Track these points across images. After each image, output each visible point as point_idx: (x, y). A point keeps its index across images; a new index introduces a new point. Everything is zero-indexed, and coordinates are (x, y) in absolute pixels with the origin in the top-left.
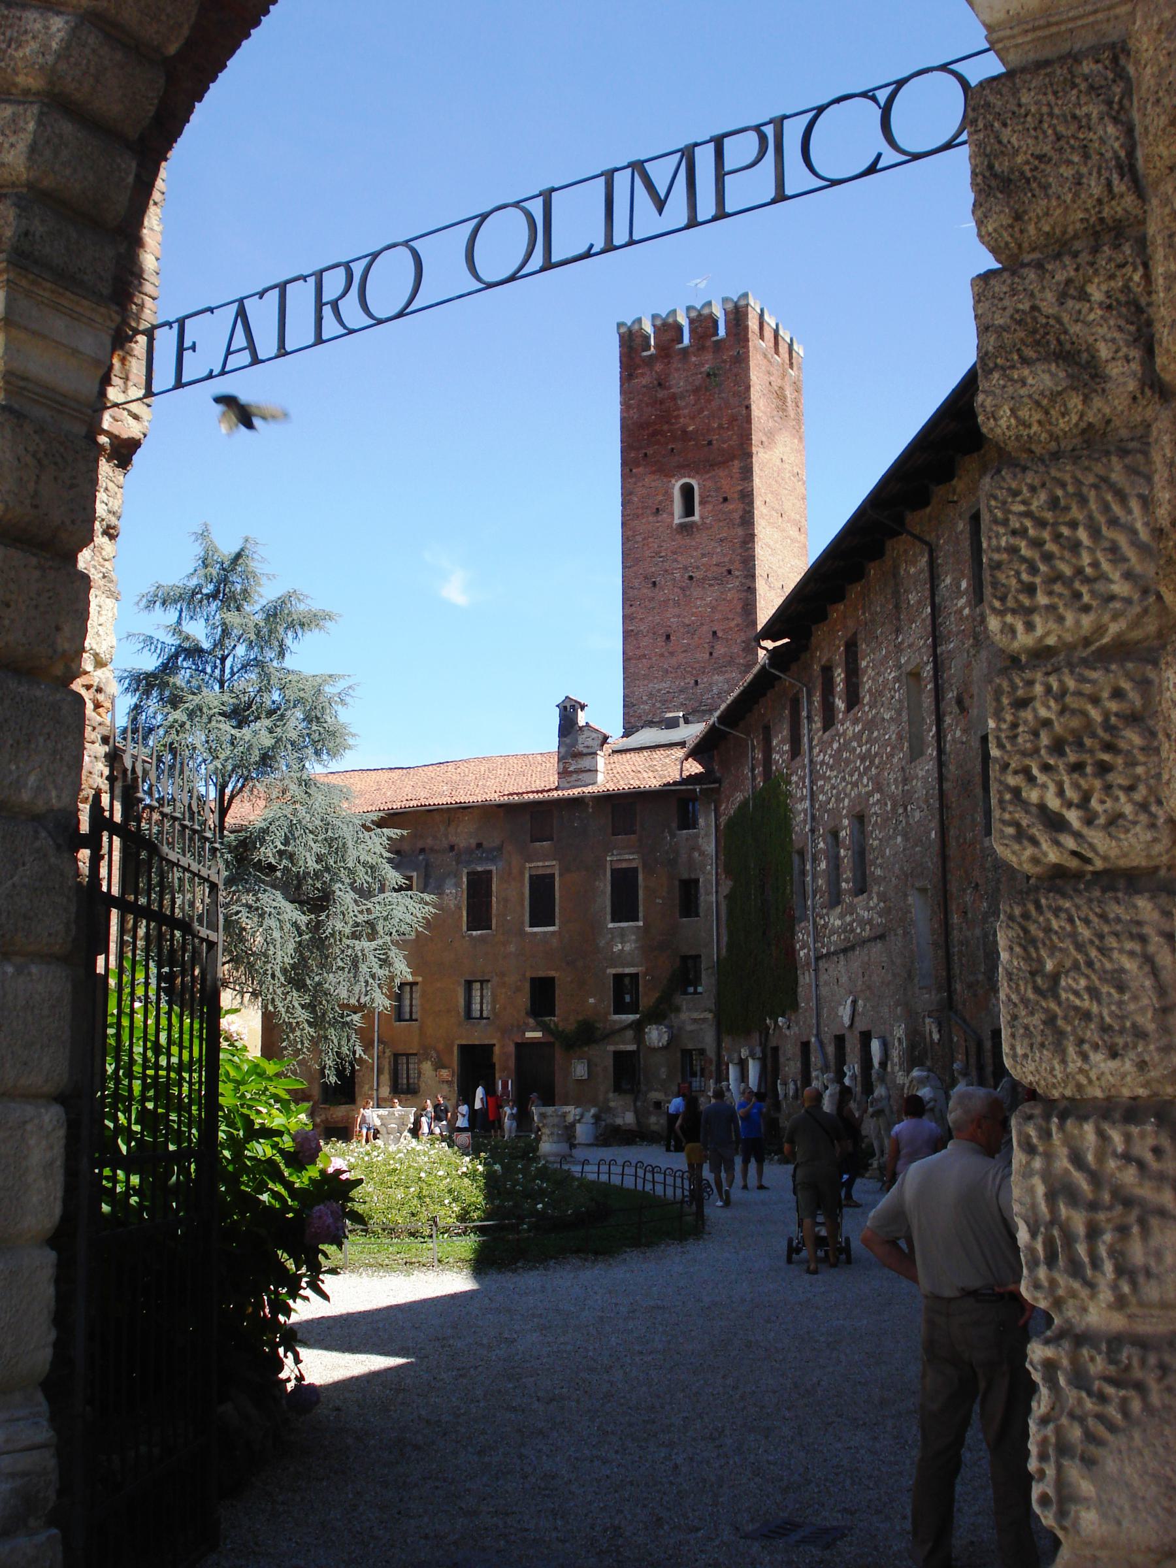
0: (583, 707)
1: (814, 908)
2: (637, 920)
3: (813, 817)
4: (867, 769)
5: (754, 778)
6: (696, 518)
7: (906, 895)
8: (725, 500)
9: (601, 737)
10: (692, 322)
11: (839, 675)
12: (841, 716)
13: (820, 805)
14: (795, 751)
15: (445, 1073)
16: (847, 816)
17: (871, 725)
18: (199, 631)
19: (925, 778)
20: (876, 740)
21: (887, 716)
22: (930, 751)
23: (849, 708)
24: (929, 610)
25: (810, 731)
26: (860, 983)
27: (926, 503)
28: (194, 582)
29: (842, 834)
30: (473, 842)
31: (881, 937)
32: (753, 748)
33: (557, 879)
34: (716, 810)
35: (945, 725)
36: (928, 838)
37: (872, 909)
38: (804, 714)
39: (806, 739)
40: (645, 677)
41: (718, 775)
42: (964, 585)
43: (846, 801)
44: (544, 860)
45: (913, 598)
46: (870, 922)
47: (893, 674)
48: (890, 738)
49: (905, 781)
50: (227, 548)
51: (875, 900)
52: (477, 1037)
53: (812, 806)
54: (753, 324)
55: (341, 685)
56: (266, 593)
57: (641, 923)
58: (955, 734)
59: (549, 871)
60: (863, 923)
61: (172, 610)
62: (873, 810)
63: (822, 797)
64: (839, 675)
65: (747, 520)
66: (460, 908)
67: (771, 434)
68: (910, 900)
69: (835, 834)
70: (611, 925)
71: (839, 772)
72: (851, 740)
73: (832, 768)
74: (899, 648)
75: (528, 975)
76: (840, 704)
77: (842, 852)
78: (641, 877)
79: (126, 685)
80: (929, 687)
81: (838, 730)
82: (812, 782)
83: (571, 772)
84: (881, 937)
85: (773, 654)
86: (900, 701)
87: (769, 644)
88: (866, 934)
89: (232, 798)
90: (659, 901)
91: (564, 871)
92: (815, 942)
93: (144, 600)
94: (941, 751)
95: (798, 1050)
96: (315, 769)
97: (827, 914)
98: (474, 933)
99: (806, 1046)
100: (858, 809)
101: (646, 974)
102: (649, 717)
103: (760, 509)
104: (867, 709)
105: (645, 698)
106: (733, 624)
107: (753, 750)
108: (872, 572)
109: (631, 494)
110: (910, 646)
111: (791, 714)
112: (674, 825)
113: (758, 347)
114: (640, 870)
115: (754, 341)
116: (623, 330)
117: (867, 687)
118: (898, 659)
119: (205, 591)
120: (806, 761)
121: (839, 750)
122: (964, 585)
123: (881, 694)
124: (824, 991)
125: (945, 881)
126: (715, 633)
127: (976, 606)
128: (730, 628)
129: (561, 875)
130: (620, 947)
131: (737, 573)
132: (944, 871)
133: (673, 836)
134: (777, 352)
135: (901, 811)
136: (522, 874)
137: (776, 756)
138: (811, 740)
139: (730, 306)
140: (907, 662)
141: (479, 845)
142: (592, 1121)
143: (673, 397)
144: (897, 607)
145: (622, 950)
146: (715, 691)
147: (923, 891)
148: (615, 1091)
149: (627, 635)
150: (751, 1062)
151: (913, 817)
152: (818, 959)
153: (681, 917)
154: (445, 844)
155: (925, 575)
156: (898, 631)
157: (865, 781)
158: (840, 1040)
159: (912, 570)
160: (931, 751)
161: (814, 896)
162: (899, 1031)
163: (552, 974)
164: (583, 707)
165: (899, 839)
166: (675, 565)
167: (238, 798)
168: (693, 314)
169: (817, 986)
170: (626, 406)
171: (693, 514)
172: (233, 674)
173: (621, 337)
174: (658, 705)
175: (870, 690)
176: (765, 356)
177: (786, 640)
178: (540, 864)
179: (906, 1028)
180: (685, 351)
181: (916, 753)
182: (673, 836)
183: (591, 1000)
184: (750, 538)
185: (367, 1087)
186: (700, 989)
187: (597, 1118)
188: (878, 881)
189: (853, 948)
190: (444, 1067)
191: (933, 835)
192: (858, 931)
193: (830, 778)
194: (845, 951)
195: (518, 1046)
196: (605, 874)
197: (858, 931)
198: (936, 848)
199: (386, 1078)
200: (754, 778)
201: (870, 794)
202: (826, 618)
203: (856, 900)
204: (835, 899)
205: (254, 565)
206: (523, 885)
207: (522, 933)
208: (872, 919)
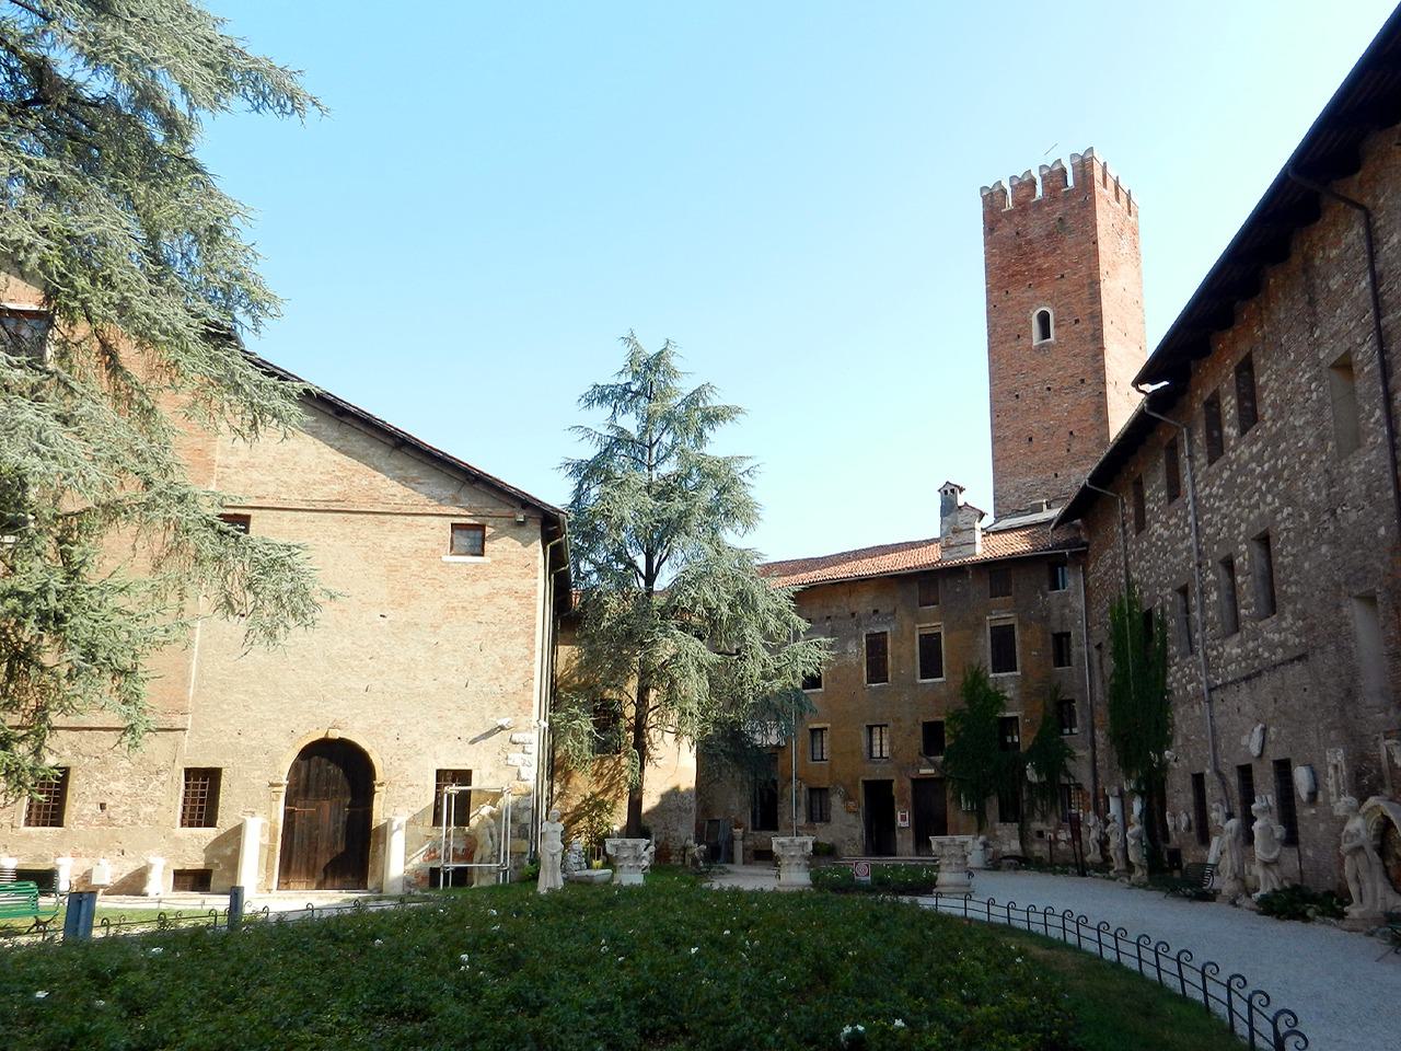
0: (961, 490)
1: (1204, 641)
3: (1200, 552)
4: (1275, 484)
5: (1125, 533)
6: (1052, 339)
7: (1338, 607)
8: (1077, 321)
10: (1044, 178)
11: (1229, 406)
12: (1232, 443)
14: (1174, 490)
16: (1245, 541)
17: (1274, 440)
18: (630, 423)
19: (1366, 473)
20: (1284, 452)
21: (1299, 422)
23: (1243, 431)
25: (1192, 470)
26: (1271, 709)
27: (1356, 169)
28: (623, 380)
29: (1238, 561)
30: (871, 609)
31: (1301, 658)
32: (1123, 505)
33: (943, 637)
37: (1284, 630)
39: (1187, 479)
40: (1011, 474)
41: (1085, 540)
43: (1243, 527)
45: (1335, 283)
46: (1282, 644)
48: (1305, 444)
49: (1331, 483)
50: (650, 349)
51: (1290, 620)
52: (878, 773)
53: (1198, 543)
54: (1098, 175)
55: (747, 465)
56: (685, 386)
57: (1019, 673)
60: (1272, 647)
61: (608, 407)
62: (1282, 526)
64: (1229, 406)
65: (1097, 337)
66: (861, 664)
67: (1114, 265)
70: (992, 675)
71: (1233, 499)
72: (1247, 463)
73: (1221, 499)
74: (1317, 344)
77: (1239, 579)
78: (1017, 633)
79: (570, 470)
82: (1196, 519)
84: (1301, 658)
85: (1153, 399)
87: (1149, 388)
89: (660, 564)
90: (1033, 653)
92: (1208, 673)
93: (583, 400)
95: (1189, 782)
96: (731, 537)
97: (1222, 645)
99: (1198, 780)
100: (1260, 530)
103: (1107, 329)
105: (1012, 491)
106: (1087, 424)
107: (1123, 507)
108: (1272, 281)
111: (1167, 462)
112: (1046, 587)
113: (1103, 195)
114: (1016, 627)
115: (1098, 187)
117: (1268, 401)
119: (634, 388)
121: (1231, 477)
124: (1220, 722)
128: (1084, 428)
131: (1090, 382)
133: (1045, 595)
134: (1118, 199)
137: (1149, 506)
138: (1193, 478)
139: (1077, 160)
141: (876, 612)
142: (982, 847)
143: (1030, 242)
144: (1312, 302)
146: (1073, 481)
147: (1369, 599)
148: (1001, 821)
149: (996, 440)
151: (1346, 519)
152: (1210, 690)
153: (1056, 666)
156: (1313, 326)
157: (1269, 498)
158: (1245, 772)
161: (1204, 629)
162: (1337, 756)
164: (961, 490)
167: (666, 563)
168: (1045, 172)
169: (1211, 717)
170: (989, 256)
171: (1049, 337)
173: (984, 198)
174: (1024, 496)
175: (1273, 405)
177: (1165, 383)
178: (928, 625)
179: (1347, 754)
180: (1039, 204)
182: (1045, 595)
184: (1100, 351)
185: (787, 817)
186: (1075, 730)
187: (985, 845)
188: (1292, 599)
189: (1259, 674)
190: (852, 800)
193: (1219, 508)
194: (1247, 678)
196: (985, 632)
199: (803, 810)
200: (1125, 533)
201: (1276, 512)
202: (1210, 352)
204: (1236, 626)
205: (675, 362)
206: (914, 642)
207: (915, 685)
208: (1286, 640)
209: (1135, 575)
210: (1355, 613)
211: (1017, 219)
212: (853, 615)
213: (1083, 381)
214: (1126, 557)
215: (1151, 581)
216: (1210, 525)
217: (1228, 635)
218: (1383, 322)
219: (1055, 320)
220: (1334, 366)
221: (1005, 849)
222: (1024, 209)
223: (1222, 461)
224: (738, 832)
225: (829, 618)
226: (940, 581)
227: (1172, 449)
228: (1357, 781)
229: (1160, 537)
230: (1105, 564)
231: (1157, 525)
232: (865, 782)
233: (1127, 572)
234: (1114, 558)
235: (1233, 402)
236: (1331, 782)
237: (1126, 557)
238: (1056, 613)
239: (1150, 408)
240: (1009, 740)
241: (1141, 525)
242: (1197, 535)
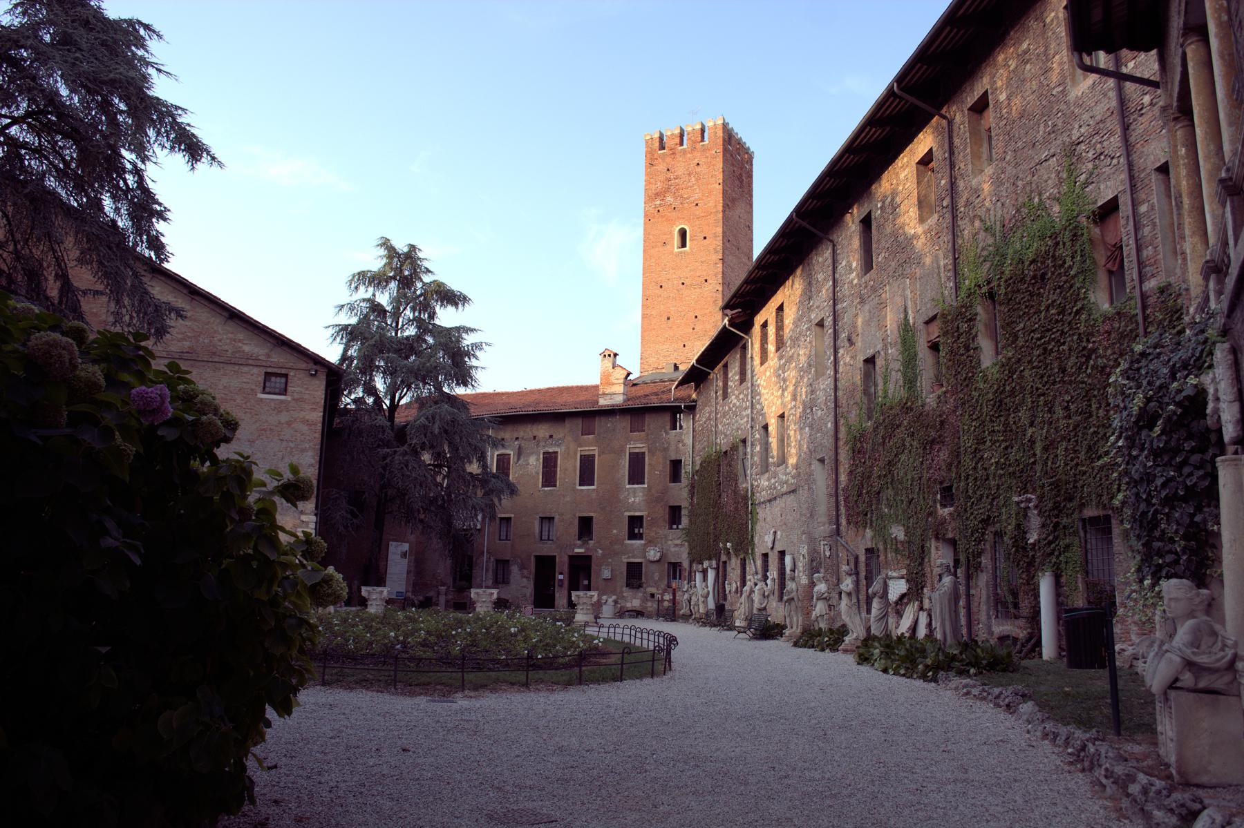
0: (616, 355)
1: (751, 475)
2: (644, 483)
3: (753, 419)
5: (717, 398)
6: (687, 248)
7: (810, 464)
8: (705, 238)
9: (626, 373)
11: (771, 330)
12: (772, 355)
13: (757, 412)
14: (743, 379)
15: (525, 572)
19: (824, 389)
22: (829, 372)
24: (831, 283)
29: (770, 428)
30: (547, 435)
31: (793, 491)
34: (693, 419)
35: (839, 355)
36: (826, 427)
37: (788, 474)
38: (749, 356)
42: (854, 264)
43: (774, 407)
44: (589, 446)
45: (820, 277)
46: (786, 482)
47: (806, 326)
49: (812, 392)
52: (546, 549)
53: (752, 412)
58: (845, 358)
59: (591, 453)
60: (783, 483)
63: (758, 407)
64: (771, 330)
68: (813, 467)
69: (766, 427)
70: (628, 486)
75: (577, 515)
76: (771, 348)
80: (829, 332)
81: (769, 364)
82: (752, 397)
83: (607, 394)
84: (793, 491)
86: (810, 342)
88: (785, 489)
91: (601, 453)
94: (836, 371)
98: (546, 489)
100: (781, 412)
101: (648, 516)
102: (656, 366)
104: (788, 349)
107: (717, 381)
109: (649, 234)
110: (818, 307)
112: (668, 427)
114: (647, 454)
116: (648, 138)
118: (810, 316)
120: (749, 385)
122: (854, 264)
123: (798, 339)
125: (837, 454)
126: (696, 317)
127: (862, 277)
129: (599, 456)
130: (633, 499)
132: (836, 448)
133: (667, 433)
135: (808, 411)
136: (576, 454)
137: (730, 383)
140: (815, 318)
141: (551, 436)
145: (634, 502)
147: (822, 461)
148: (627, 586)
149: (644, 316)
150: (709, 570)
154: (531, 436)
155: (830, 261)
159: (820, 260)
160: (831, 372)
161: (752, 468)
162: (804, 550)
163: (591, 514)
165: (807, 429)
166: (674, 276)
172: (403, 326)
176: (732, 155)
178: (587, 448)
180: (684, 151)
181: (818, 375)
182: (667, 433)
183: (615, 531)
187: (616, 602)
189: (775, 498)
190: (525, 568)
191: (829, 425)
192: (779, 488)
194: (770, 501)
195: (571, 557)
196: (625, 456)
197: (779, 488)
198: (832, 432)
200: (717, 398)
203: (778, 469)
207: (574, 490)
209: (720, 427)
210: (816, 466)
211: (668, 159)
212: (535, 437)
213: (706, 281)
214: (716, 414)
215: (728, 432)
216: (758, 403)
217: (762, 473)
218: (839, 307)
219: (691, 236)
220: (816, 324)
221: (629, 605)
222: (673, 154)
223: (766, 365)
224: (443, 588)
225: (517, 439)
226: (597, 418)
227: (744, 348)
228: (811, 564)
229: (734, 404)
230: (703, 415)
231: (734, 397)
232: (537, 557)
233: (716, 425)
234: (710, 413)
235: (774, 330)
236: (801, 565)
237: (716, 414)
238: (673, 447)
239: (729, 325)
240: (636, 531)
241: (725, 396)
242: (752, 408)
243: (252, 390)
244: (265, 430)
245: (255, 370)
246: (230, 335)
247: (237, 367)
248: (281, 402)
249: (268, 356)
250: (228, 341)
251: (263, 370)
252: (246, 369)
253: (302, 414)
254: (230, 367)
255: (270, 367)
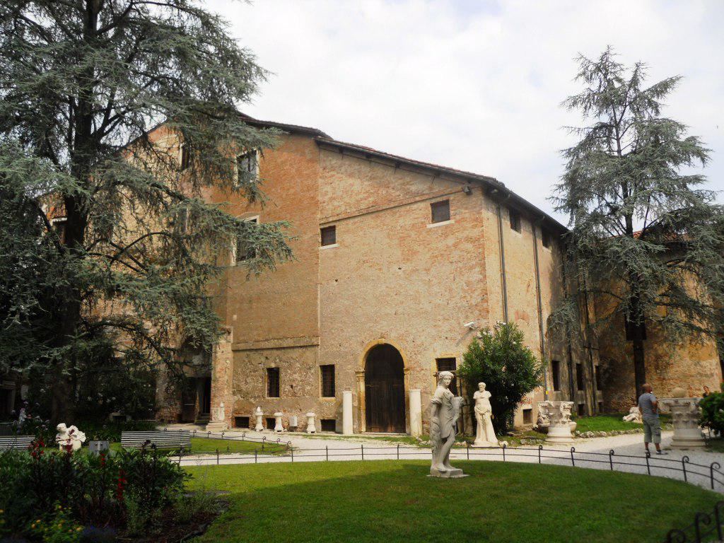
243: (422, 223)
244: (436, 257)
245: (422, 205)
246: (400, 181)
247: (408, 207)
248: (447, 227)
249: (431, 189)
250: (399, 187)
251: (428, 204)
252: (415, 206)
253: (466, 233)
254: (403, 209)
255: (434, 198)
